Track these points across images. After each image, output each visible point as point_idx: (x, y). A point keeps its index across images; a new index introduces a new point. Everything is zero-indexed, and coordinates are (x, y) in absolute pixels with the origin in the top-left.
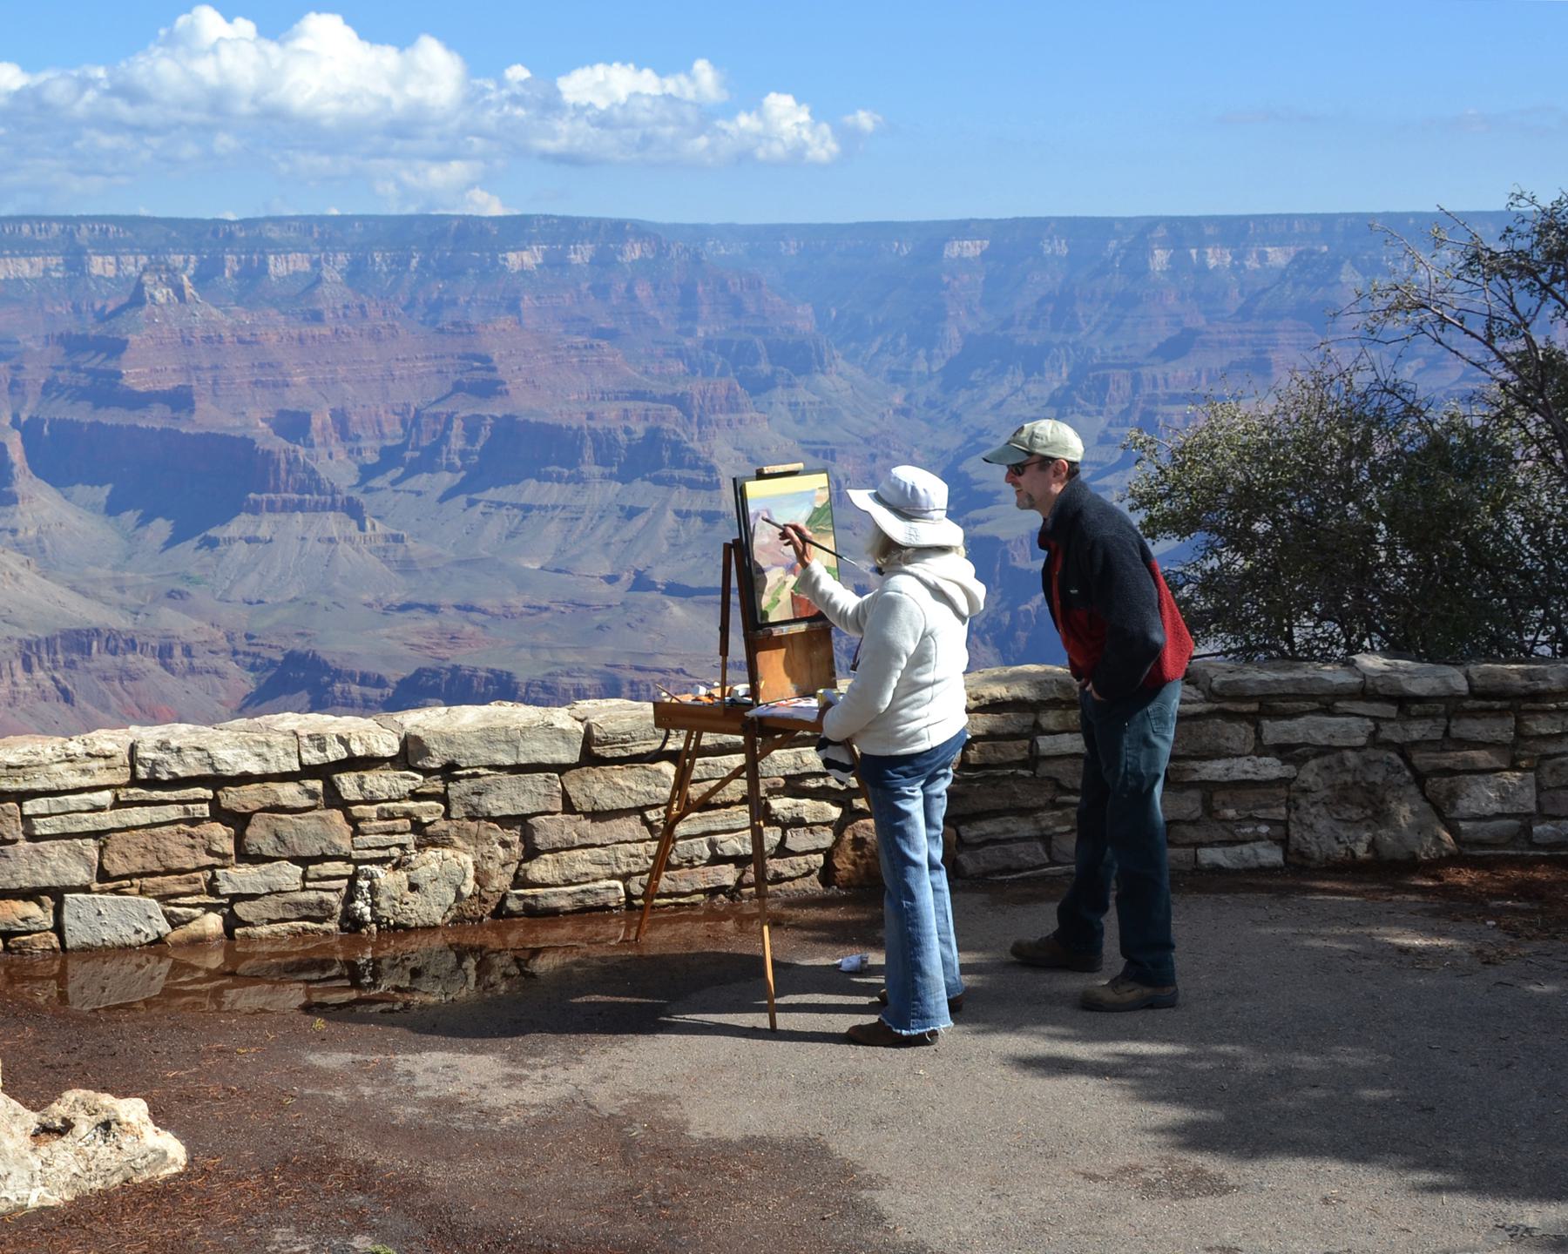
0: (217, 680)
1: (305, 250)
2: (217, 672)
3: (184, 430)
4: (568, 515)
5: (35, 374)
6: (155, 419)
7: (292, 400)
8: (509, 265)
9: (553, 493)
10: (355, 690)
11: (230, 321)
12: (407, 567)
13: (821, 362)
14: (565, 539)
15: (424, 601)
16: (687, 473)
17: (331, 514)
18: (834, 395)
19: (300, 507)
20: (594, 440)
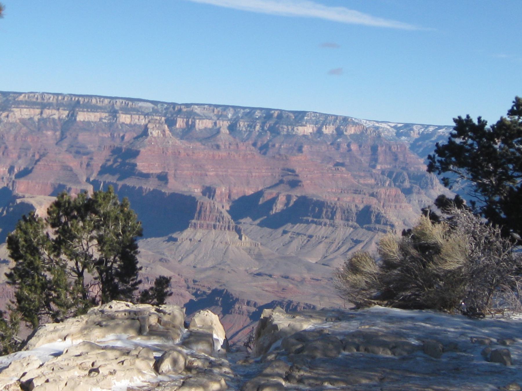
1: (211, 119)
2: (181, 295)
3: (163, 191)
5: (98, 162)
6: (149, 186)
7: (208, 182)
9: (322, 231)
10: (245, 307)
11: (183, 146)
12: (259, 257)
13: (432, 184)
14: (327, 251)
15: (267, 273)
16: (381, 227)
20: (341, 209)
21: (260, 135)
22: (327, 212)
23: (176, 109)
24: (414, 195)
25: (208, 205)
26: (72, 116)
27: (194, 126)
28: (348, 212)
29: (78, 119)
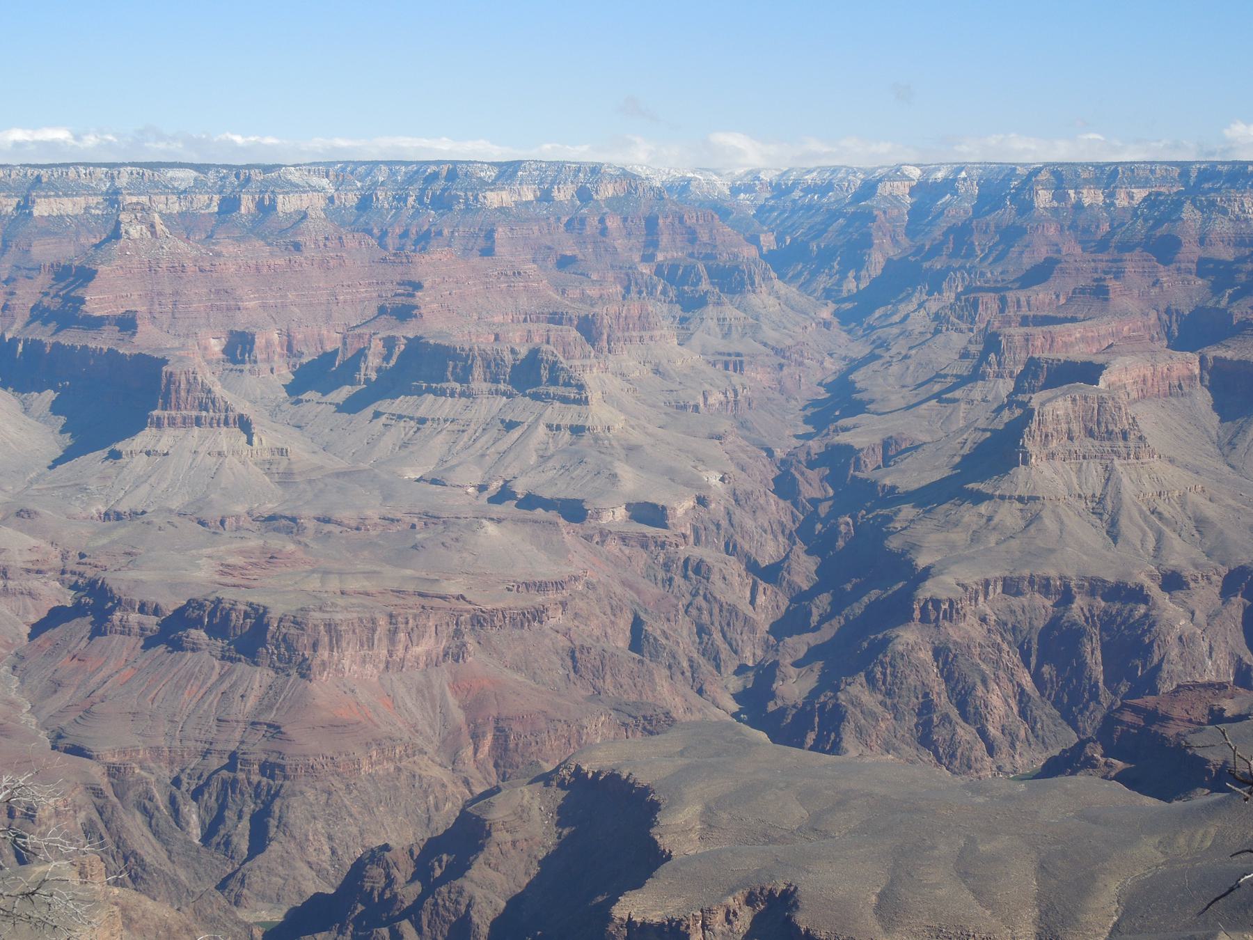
0: (29, 601)
2: (30, 594)
3: (121, 351)
4: (456, 427)
6: (102, 341)
7: (241, 323)
8: (488, 203)
9: (446, 407)
12: (286, 479)
13: (752, 284)
14: (449, 450)
15: (288, 513)
16: (560, 390)
17: (224, 429)
18: (763, 312)
19: (198, 422)
21: (417, 213)
22: (455, 367)
23: (242, 177)
24: (710, 307)
25: (183, 378)
26: (25, 206)
27: (275, 209)
28: (497, 365)
29: (36, 213)
